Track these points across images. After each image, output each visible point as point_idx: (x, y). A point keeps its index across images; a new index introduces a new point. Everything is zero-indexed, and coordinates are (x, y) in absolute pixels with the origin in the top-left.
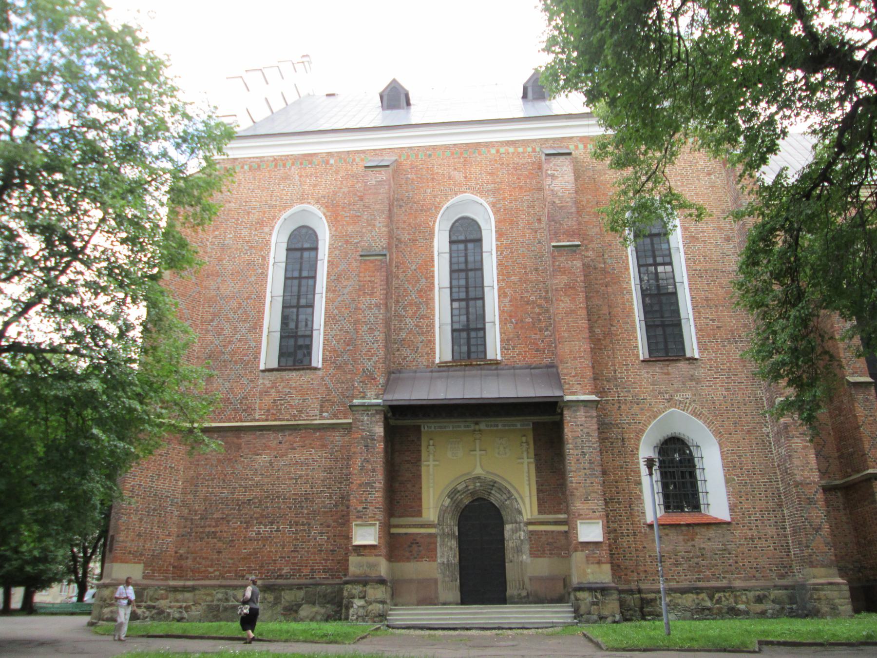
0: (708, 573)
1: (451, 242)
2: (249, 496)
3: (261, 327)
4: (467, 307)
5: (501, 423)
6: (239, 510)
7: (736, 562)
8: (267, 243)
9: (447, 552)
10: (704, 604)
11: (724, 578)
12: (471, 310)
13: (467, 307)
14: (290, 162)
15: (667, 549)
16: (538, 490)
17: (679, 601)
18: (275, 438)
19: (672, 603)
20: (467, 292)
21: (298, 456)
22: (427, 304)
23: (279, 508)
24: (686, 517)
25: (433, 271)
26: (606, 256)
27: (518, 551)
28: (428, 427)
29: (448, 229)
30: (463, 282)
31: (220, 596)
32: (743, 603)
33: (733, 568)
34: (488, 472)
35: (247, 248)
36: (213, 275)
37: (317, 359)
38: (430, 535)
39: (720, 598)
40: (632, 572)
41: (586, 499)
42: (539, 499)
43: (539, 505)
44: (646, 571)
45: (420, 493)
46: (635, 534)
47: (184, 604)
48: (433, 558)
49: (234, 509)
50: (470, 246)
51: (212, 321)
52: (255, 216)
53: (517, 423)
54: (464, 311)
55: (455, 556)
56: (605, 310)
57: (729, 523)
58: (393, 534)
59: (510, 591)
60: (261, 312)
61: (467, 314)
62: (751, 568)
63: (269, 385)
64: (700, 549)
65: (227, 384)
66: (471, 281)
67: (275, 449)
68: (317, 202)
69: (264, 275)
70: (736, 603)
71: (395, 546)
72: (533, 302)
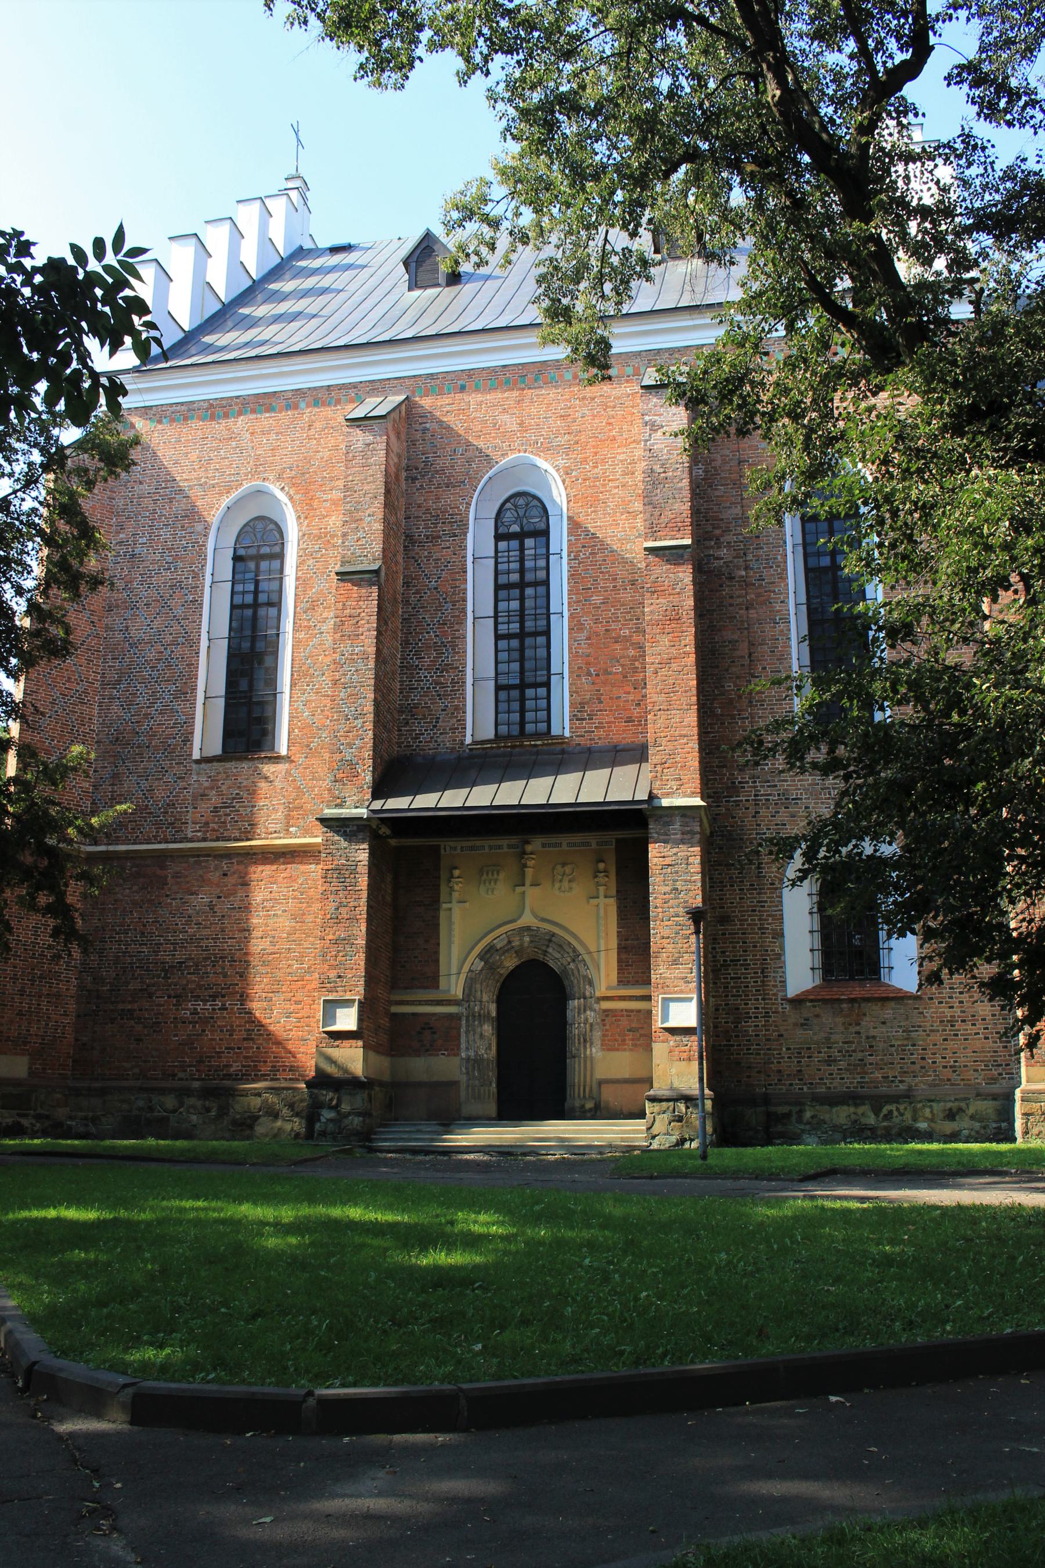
0: (878, 1075)
1: (498, 537)
2: (180, 956)
3: (194, 689)
4: (522, 649)
5: (565, 841)
6: (166, 978)
7: (923, 1059)
10: (864, 1121)
11: (901, 1082)
12: (528, 653)
13: (522, 649)
14: (236, 408)
15: (815, 1038)
16: (619, 945)
17: (827, 1117)
18: (216, 868)
19: (815, 1121)
20: (522, 623)
22: (454, 646)
23: (225, 976)
25: (466, 589)
26: (750, 557)
27: (586, 1040)
28: (450, 847)
29: (494, 516)
30: (515, 605)
31: (141, 1103)
32: (926, 1119)
33: (917, 1067)
34: (543, 920)
35: (170, 559)
36: (117, 606)
38: (450, 1016)
39: (891, 1112)
40: (759, 1072)
41: (676, 962)
42: (619, 961)
43: (620, 970)
44: (780, 1071)
45: (437, 953)
46: (767, 1015)
47: (91, 1114)
48: (455, 1051)
49: (159, 976)
50: (529, 542)
51: (119, 682)
53: (593, 839)
54: (516, 655)
55: (489, 1048)
56: (743, 649)
57: (916, 998)
58: (395, 1014)
60: (193, 666)
61: (522, 660)
62: (945, 1067)
63: (206, 784)
64: (868, 1037)
65: (144, 784)
66: (529, 603)
67: (218, 885)
68: (279, 478)
69: (197, 604)
70: (915, 1120)
72: (626, 639)
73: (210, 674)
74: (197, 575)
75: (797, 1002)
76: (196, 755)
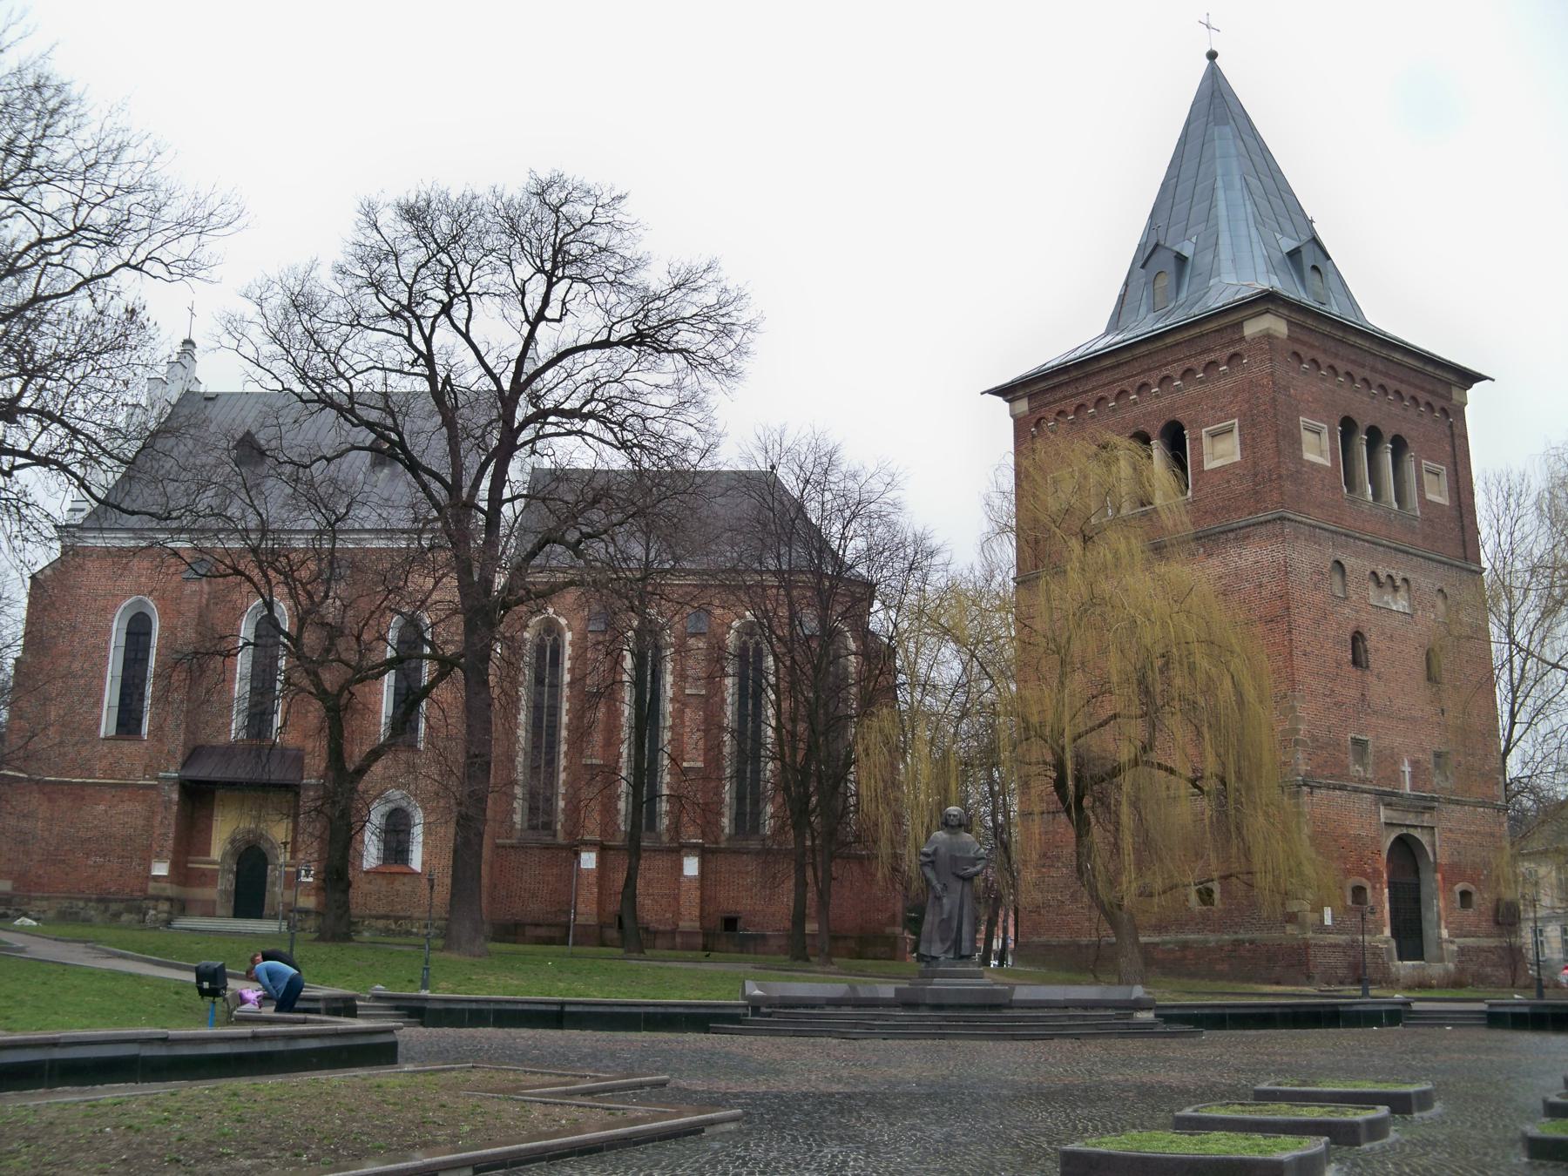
2: (90, 834)
8: (110, 630)
9: (226, 883)
21: (127, 806)
24: (395, 868)
27: (274, 884)
37: (145, 728)
52: (101, 603)
59: (266, 911)
60: (102, 690)
71: (181, 873)
73: (111, 694)
74: (107, 642)
75: (367, 872)
76: (102, 735)
